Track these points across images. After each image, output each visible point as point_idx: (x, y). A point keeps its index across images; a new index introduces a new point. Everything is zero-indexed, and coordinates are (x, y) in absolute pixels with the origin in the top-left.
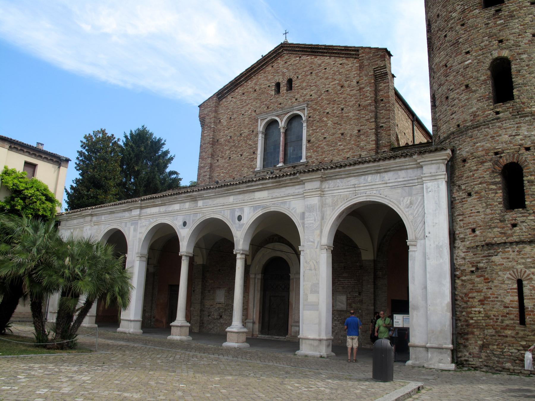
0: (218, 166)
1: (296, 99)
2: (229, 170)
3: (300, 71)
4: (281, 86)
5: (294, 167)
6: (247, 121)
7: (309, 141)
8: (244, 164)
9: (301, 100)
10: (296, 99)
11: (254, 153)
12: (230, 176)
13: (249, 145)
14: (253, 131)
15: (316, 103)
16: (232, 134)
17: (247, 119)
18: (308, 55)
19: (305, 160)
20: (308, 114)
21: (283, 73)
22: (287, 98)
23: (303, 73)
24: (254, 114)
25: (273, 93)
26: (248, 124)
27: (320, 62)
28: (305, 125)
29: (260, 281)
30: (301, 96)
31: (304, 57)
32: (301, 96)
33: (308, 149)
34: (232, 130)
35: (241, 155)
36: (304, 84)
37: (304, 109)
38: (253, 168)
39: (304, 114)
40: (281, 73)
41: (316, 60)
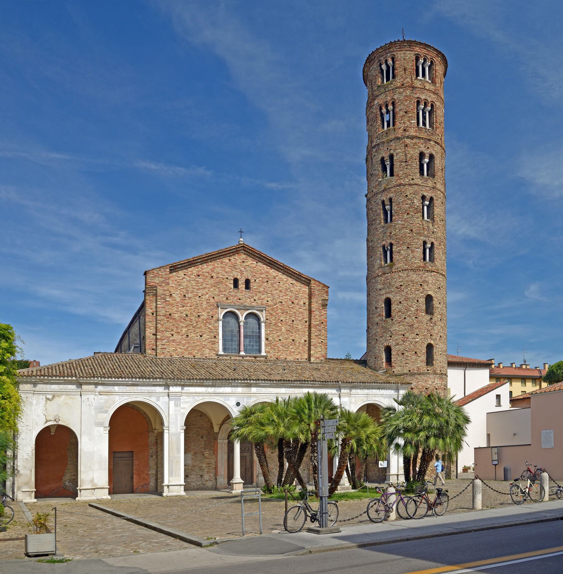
0: (173, 341)
1: (255, 300)
2: (188, 347)
3: (258, 276)
4: (240, 283)
5: (255, 357)
6: (205, 305)
7: (267, 339)
8: (206, 345)
9: (259, 302)
10: (255, 300)
11: (215, 337)
12: (190, 354)
13: (209, 328)
14: (212, 317)
15: (273, 309)
16: (188, 313)
17: (205, 303)
18: (266, 265)
19: (265, 354)
20: (266, 316)
21: (241, 270)
22: (246, 296)
23: (261, 279)
24: (212, 300)
25: (232, 286)
26: (206, 308)
27: (274, 274)
28: (263, 325)
29: (227, 445)
30: (259, 299)
31: (259, 264)
32: (259, 299)
33: (266, 345)
34: (188, 308)
35: (201, 336)
36: (262, 289)
37: (262, 311)
38: (214, 350)
39: (263, 316)
40: (239, 270)
41: (272, 271)
